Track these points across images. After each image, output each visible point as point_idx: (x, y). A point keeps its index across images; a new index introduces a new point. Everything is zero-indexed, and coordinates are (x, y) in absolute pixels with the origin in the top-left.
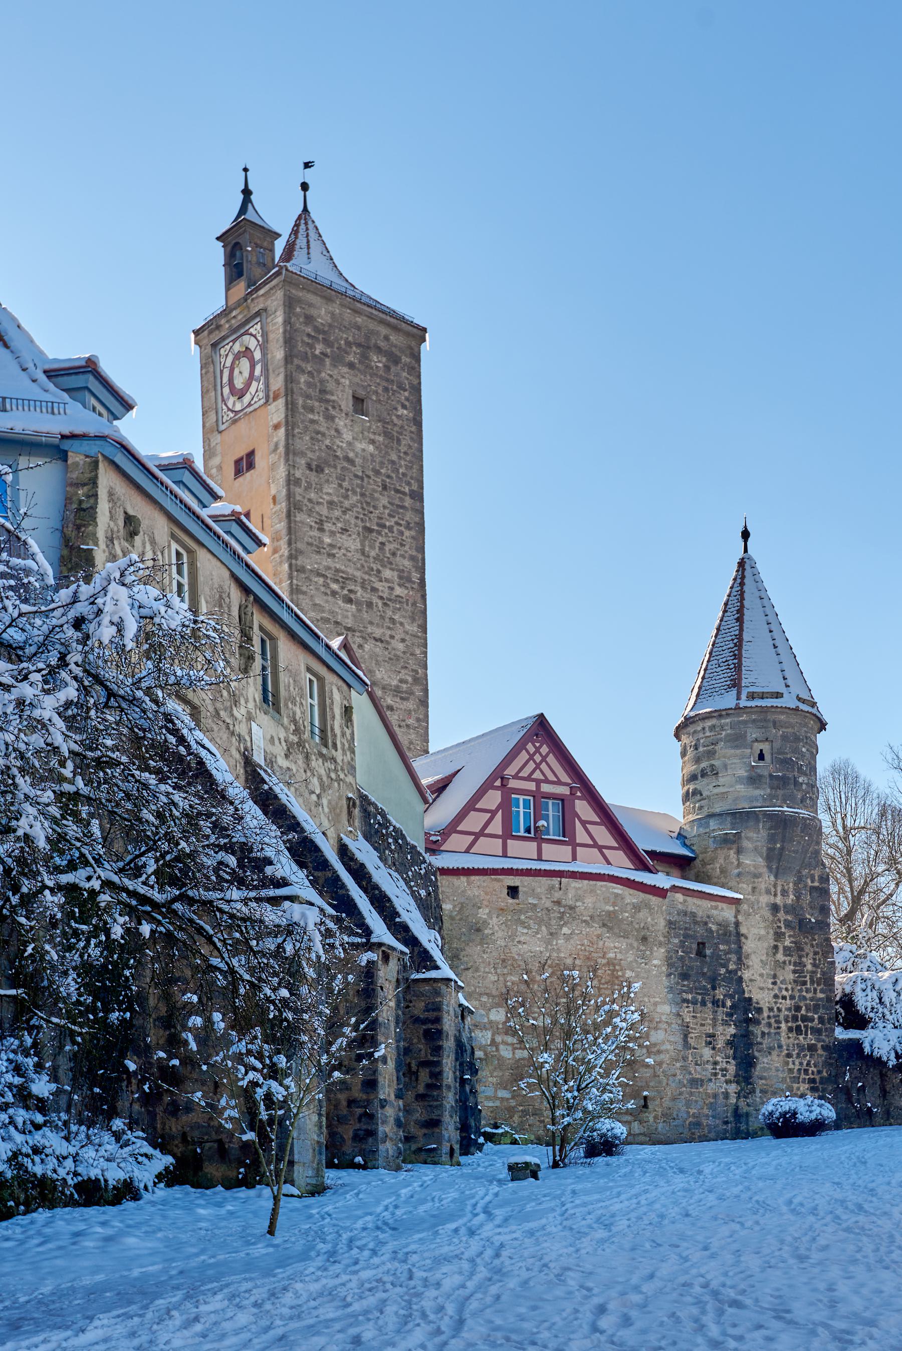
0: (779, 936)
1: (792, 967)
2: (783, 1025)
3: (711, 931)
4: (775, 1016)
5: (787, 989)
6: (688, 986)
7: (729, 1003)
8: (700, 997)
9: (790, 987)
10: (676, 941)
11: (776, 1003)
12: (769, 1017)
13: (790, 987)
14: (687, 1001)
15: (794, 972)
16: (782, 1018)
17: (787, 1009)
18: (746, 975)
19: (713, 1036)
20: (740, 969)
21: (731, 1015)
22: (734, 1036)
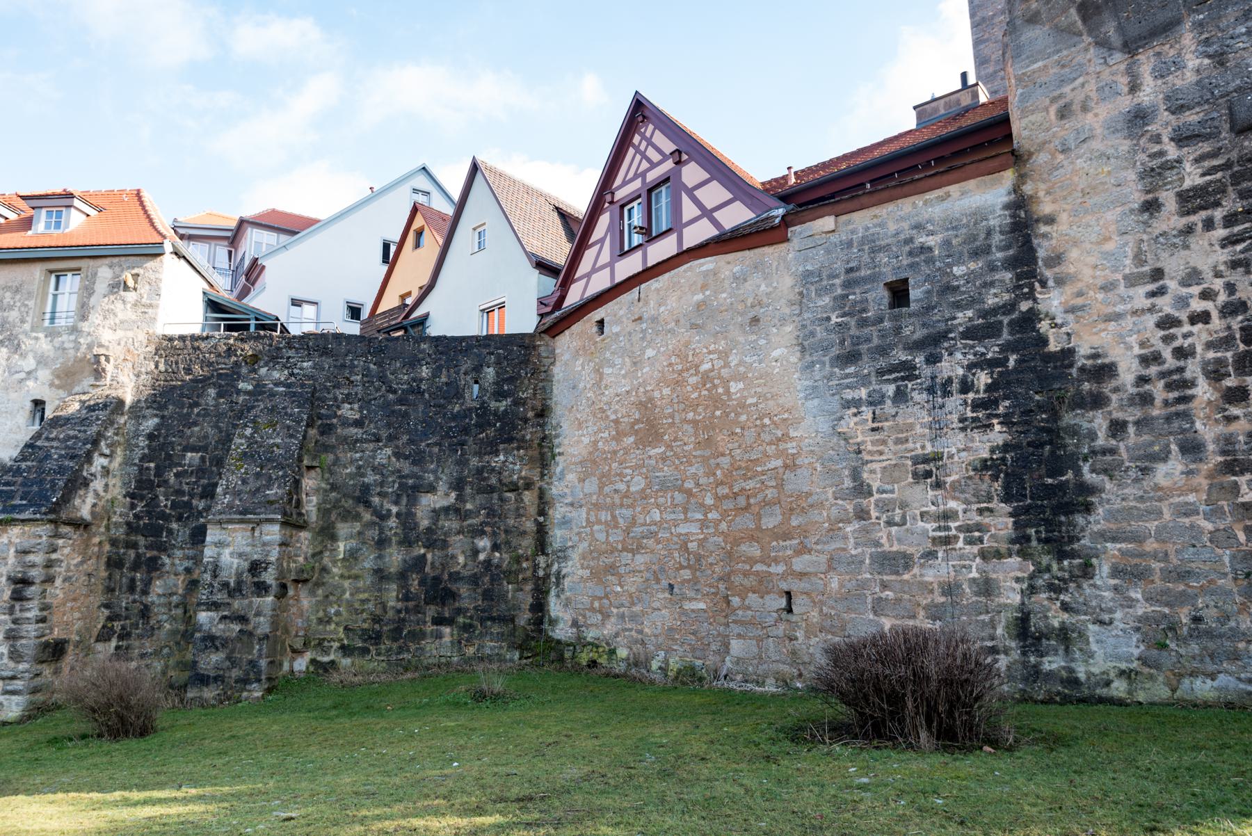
0: (1156, 173)
1: (1221, 233)
2: (1204, 391)
3: (925, 249)
4: (1162, 375)
5: (1206, 295)
6: (856, 375)
7: (983, 379)
8: (890, 389)
9: (1218, 284)
10: (827, 299)
11: (1167, 339)
12: (1142, 380)
13: (1218, 284)
14: (857, 403)
15: (1228, 242)
16: (1193, 369)
17: (1209, 345)
18: (1052, 301)
19: (937, 457)
20: (1031, 296)
21: (995, 403)
22: (1006, 447)
